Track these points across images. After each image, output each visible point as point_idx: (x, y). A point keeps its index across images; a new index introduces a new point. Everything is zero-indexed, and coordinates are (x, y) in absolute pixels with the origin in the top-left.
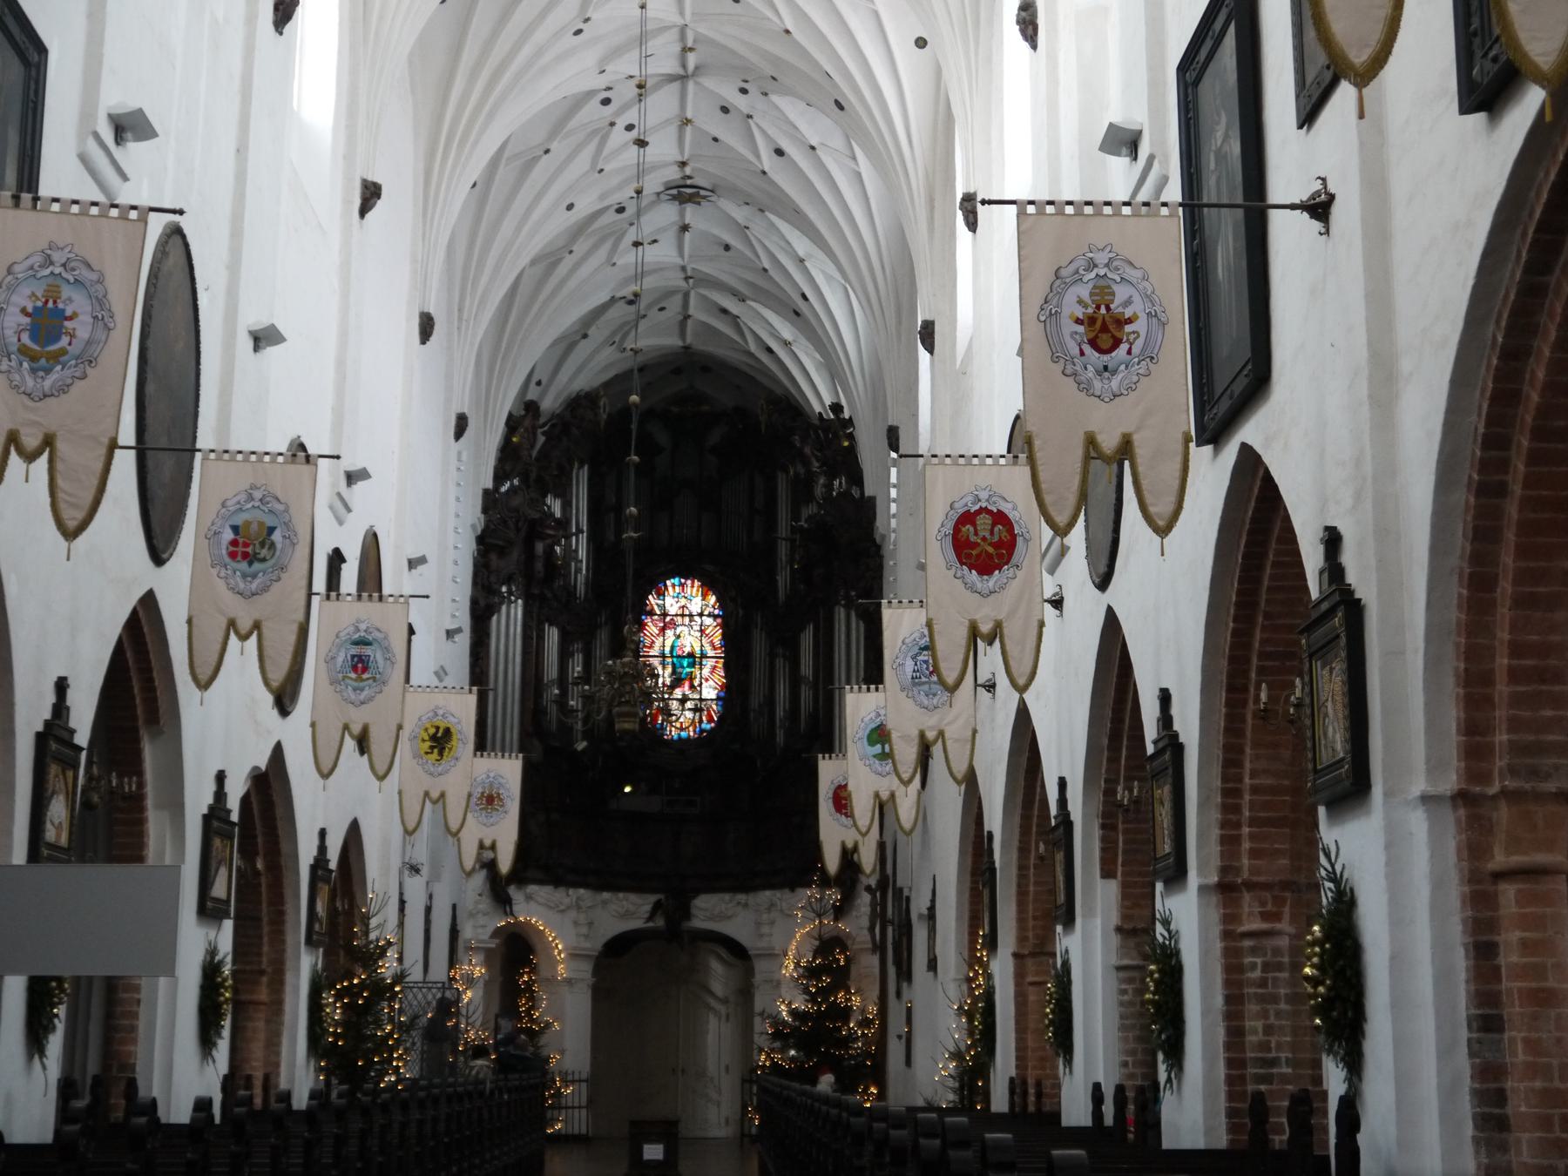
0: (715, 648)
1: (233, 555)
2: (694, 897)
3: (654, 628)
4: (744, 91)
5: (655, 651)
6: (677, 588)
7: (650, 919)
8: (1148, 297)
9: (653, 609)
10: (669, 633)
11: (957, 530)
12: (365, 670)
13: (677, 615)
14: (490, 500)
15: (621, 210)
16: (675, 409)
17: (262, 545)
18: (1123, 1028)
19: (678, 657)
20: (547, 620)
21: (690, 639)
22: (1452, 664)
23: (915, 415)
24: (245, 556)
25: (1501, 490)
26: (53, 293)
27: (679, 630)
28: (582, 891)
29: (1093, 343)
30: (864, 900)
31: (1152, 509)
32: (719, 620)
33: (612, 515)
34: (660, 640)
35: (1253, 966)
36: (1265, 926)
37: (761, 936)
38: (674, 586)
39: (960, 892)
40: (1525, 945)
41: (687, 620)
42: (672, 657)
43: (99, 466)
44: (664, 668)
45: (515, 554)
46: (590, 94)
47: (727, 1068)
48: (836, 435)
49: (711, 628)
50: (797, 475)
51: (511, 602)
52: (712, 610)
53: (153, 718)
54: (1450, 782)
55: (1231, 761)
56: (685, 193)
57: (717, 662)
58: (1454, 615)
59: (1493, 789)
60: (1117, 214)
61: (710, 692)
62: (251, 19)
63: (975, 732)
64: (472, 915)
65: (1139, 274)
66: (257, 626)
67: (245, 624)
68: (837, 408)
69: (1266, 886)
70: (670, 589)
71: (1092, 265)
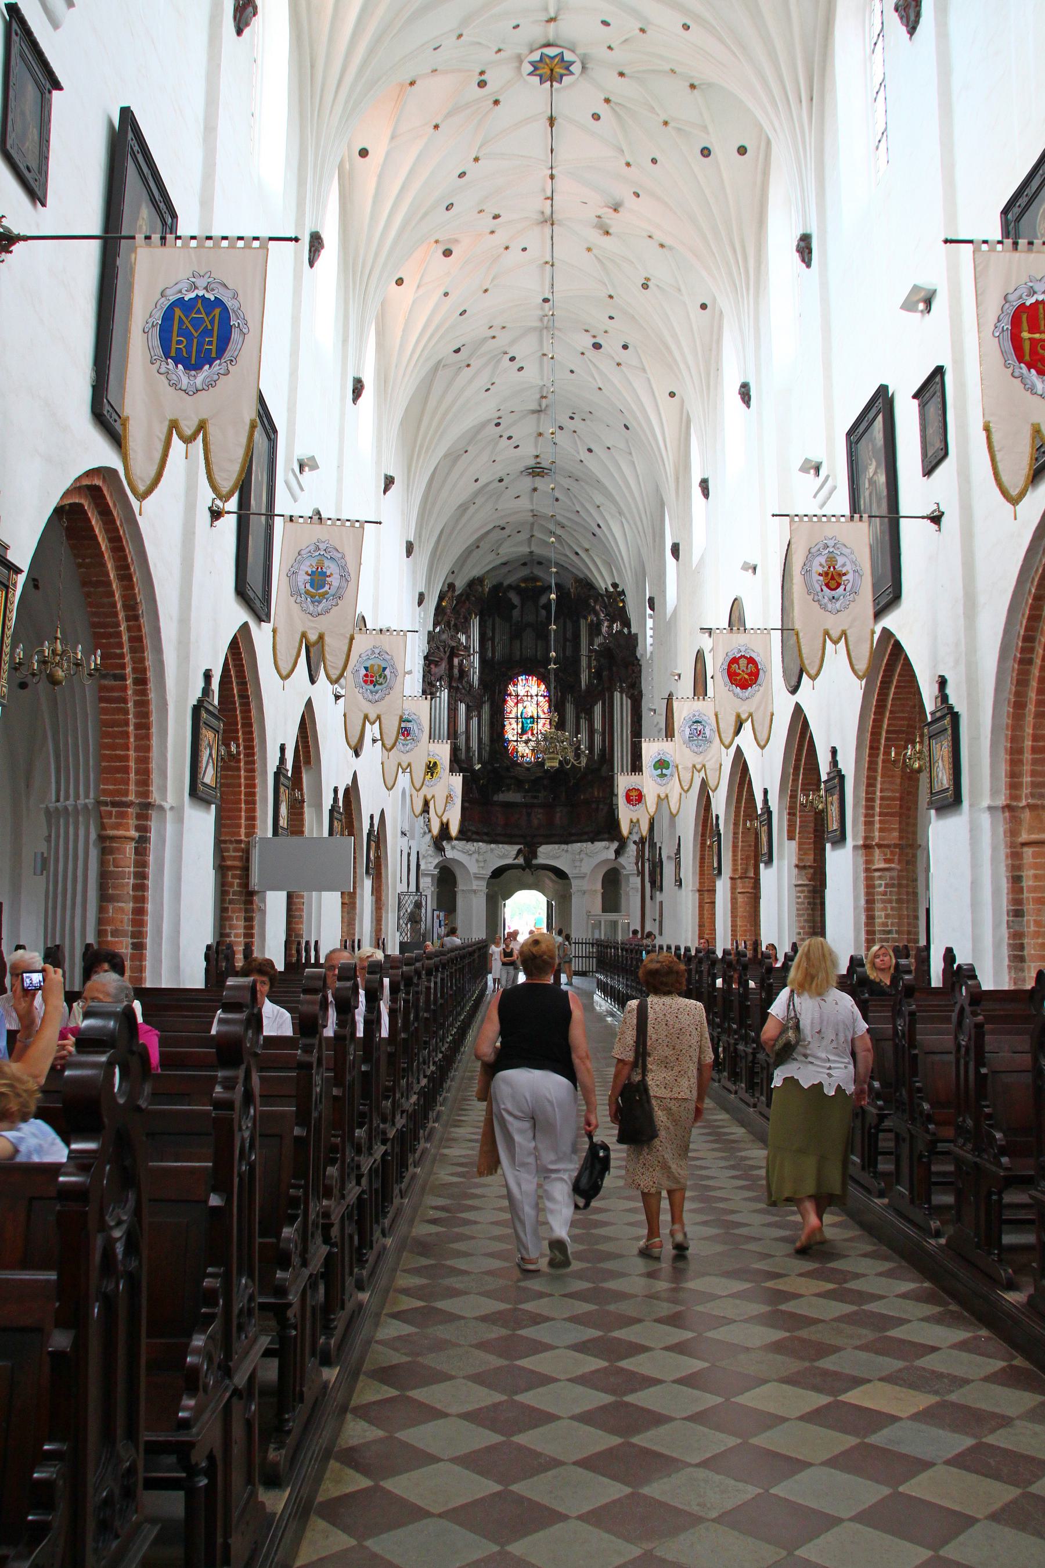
1: (365, 682)
4: (572, 418)
8: (853, 562)
11: (729, 667)
12: (408, 735)
14: (431, 637)
15: (501, 480)
16: (523, 585)
17: (380, 676)
18: (798, 915)
22: (1004, 744)
23: (664, 592)
24: (372, 682)
25: (1030, 662)
26: (320, 565)
29: (827, 585)
30: (632, 849)
31: (856, 667)
34: (514, 710)
35: (880, 886)
36: (887, 866)
39: (695, 846)
40: (1036, 877)
43: (346, 648)
45: (444, 665)
46: (489, 421)
48: (615, 600)
50: (592, 621)
53: (308, 762)
54: (1001, 801)
55: (871, 784)
56: (537, 471)
58: (1006, 720)
59: (1023, 803)
60: (838, 521)
62: (343, 399)
63: (721, 765)
64: (424, 857)
65: (849, 551)
66: (379, 717)
67: (372, 717)
68: (615, 585)
69: (888, 846)
71: (826, 546)
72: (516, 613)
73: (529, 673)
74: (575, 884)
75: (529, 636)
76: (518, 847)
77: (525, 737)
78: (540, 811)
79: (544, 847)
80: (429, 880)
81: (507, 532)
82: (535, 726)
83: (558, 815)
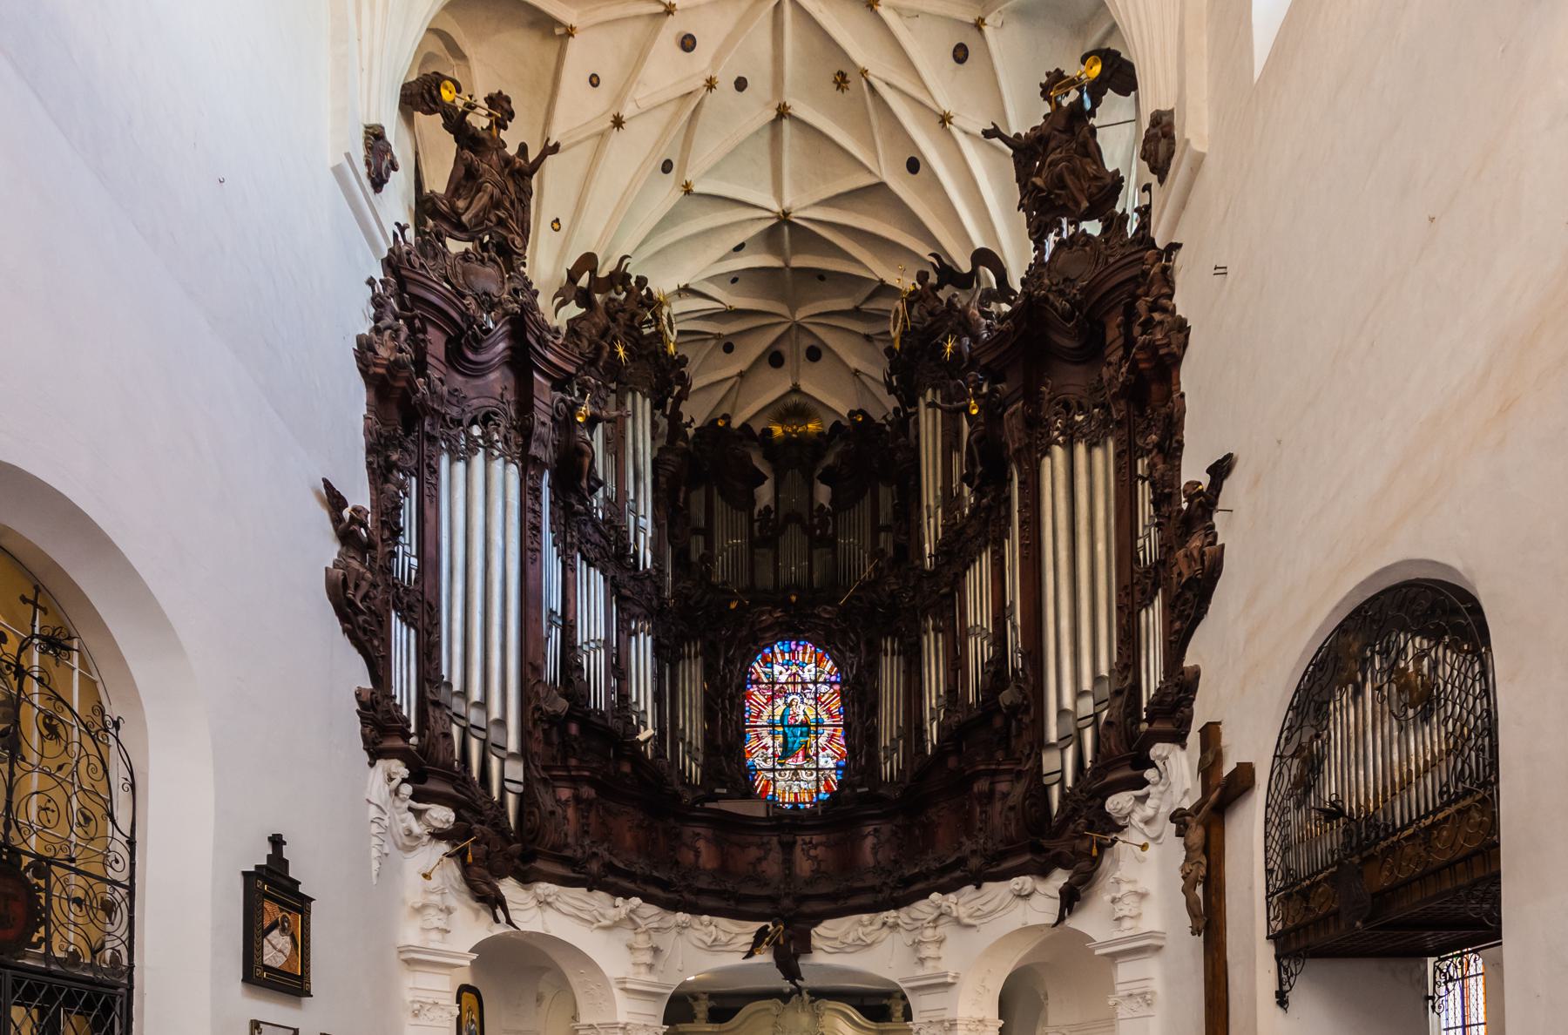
3: (761, 697)
9: (759, 677)
10: (779, 702)
13: (787, 683)
19: (789, 726)
21: (802, 707)
32: (837, 687)
33: (701, 539)
38: (783, 653)
41: (799, 688)
42: (783, 726)
44: (773, 739)
49: (827, 696)
57: (834, 730)
61: (826, 762)
70: (779, 656)
72: (765, 494)
73: (792, 630)
75: (794, 539)
76: (756, 926)
77: (791, 763)
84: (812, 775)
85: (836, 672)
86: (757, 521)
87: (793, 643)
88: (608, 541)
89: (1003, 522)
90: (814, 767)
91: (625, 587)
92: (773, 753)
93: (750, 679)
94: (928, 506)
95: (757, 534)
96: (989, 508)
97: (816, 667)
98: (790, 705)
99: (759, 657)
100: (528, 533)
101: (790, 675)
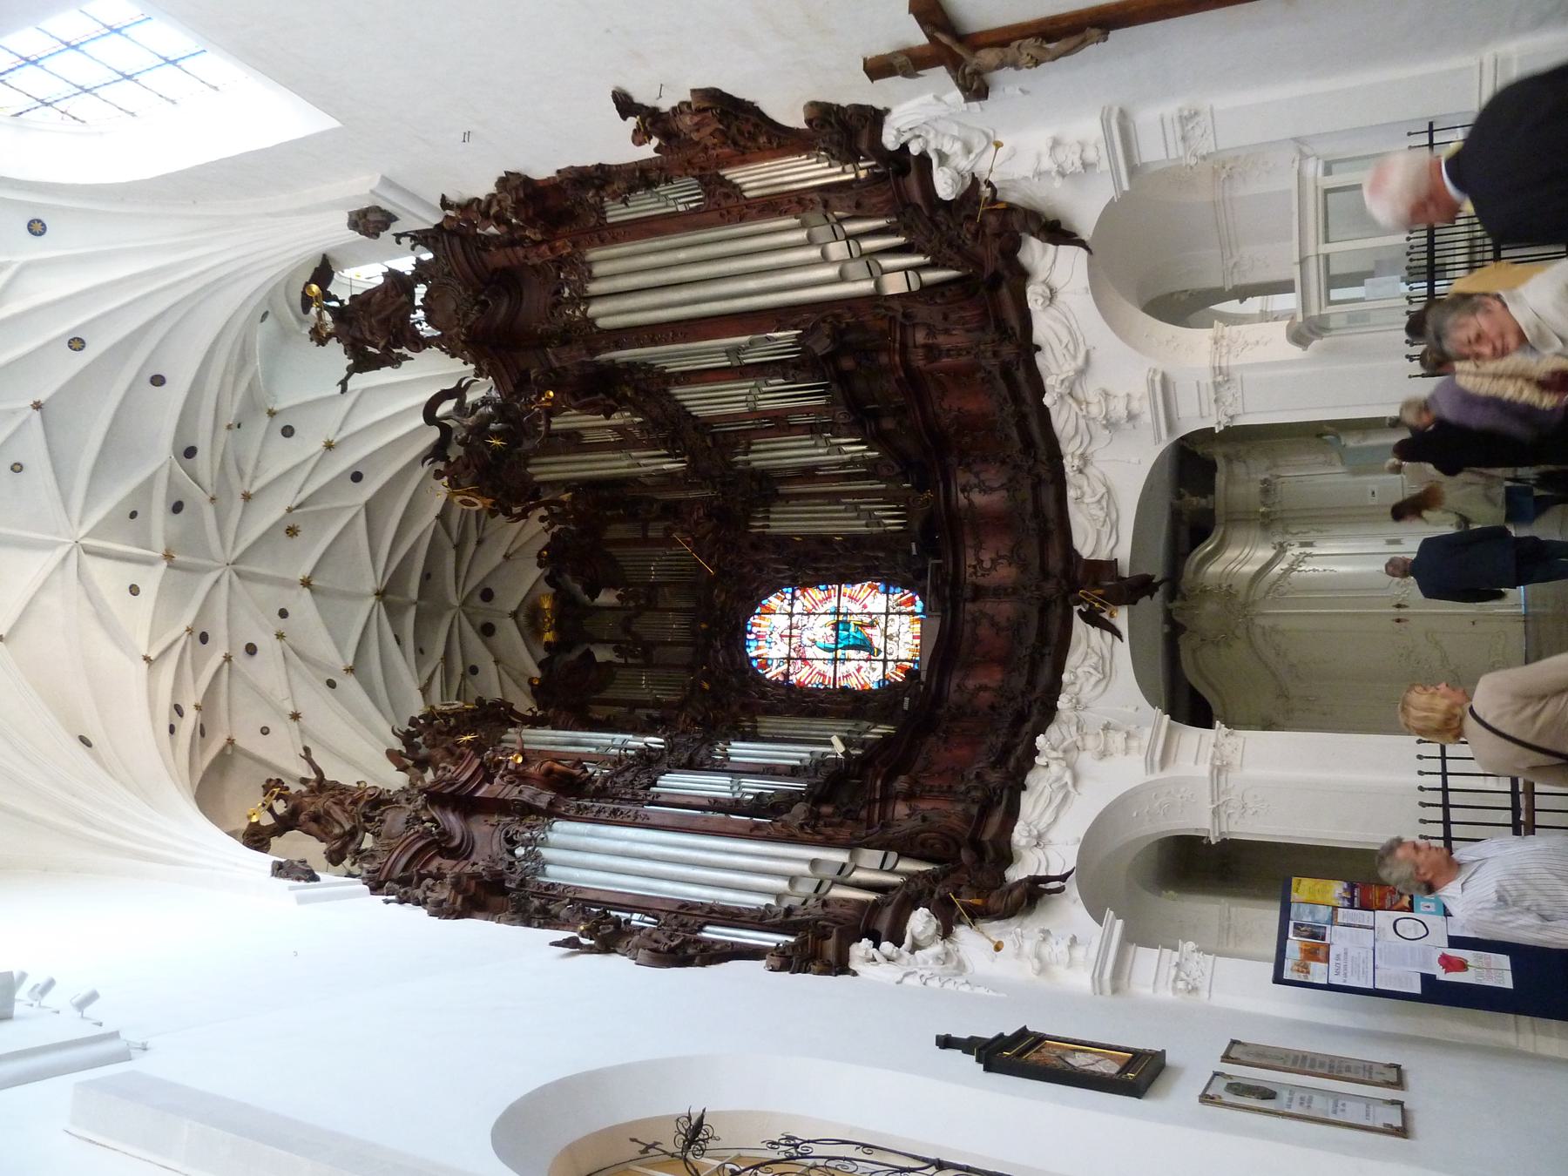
0: (830, 597)
2: (1079, 557)
5: (828, 670)
6: (761, 644)
7: (1116, 633)
10: (809, 653)
20: (647, 788)
27: (806, 642)
28: (1040, 741)
32: (798, 593)
34: (819, 666)
37: (1131, 417)
38: (758, 648)
41: (795, 632)
42: (836, 650)
47: (1390, 542)
49: (806, 603)
51: (545, 843)
52: (786, 602)
57: (845, 596)
70: (760, 652)
73: (736, 635)
74: (1196, 416)
75: (647, 624)
77: (878, 642)
78: (971, 561)
79: (1078, 542)
80: (1146, 960)
81: (266, 642)
82: (854, 619)
83: (979, 498)
84: (893, 620)
85: (782, 593)
86: (626, 661)
87: (749, 636)
88: (633, 765)
89: (650, 375)
90: (884, 616)
91: (679, 760)
92: (866, 660)
93: (783, 682)
94: (628, 467)
95: (639, 661)
96: (637, 390)
97: (774, 613)
98: (814, 642)
99: (760, 671)
100: (618, 819)
101: (782, 640)
